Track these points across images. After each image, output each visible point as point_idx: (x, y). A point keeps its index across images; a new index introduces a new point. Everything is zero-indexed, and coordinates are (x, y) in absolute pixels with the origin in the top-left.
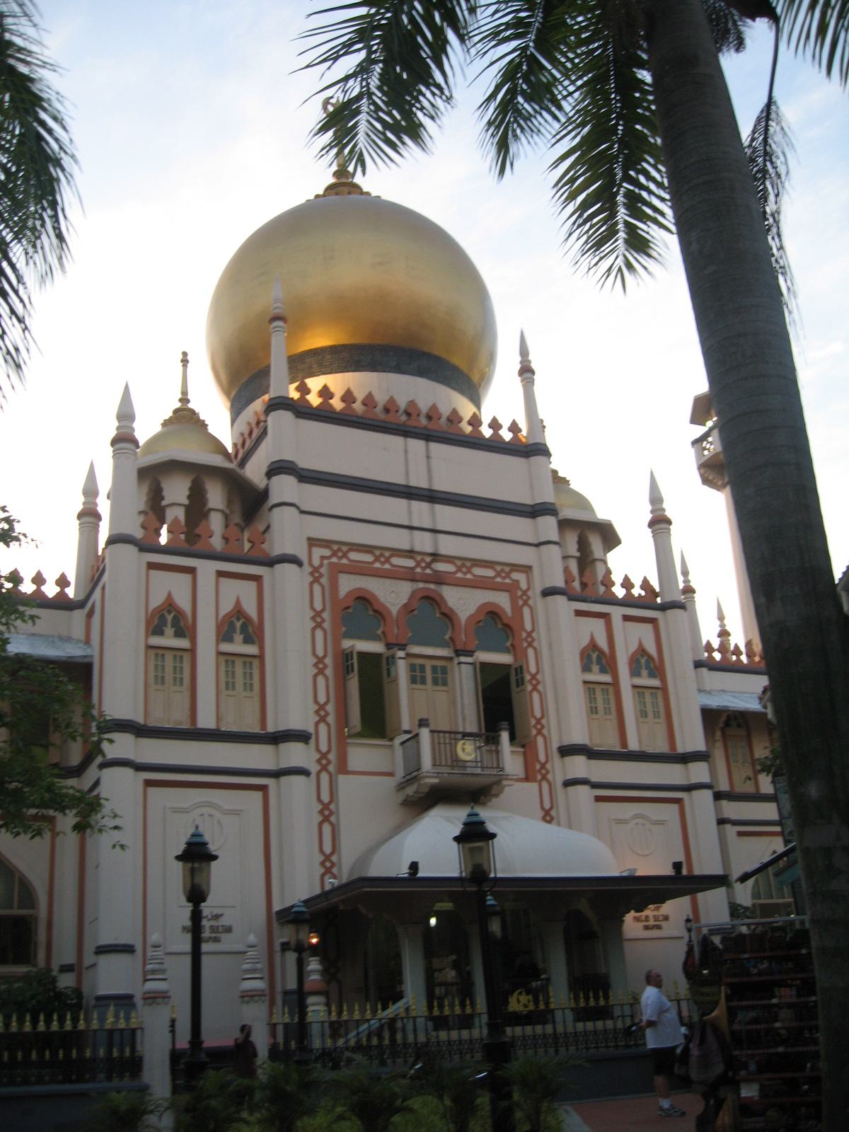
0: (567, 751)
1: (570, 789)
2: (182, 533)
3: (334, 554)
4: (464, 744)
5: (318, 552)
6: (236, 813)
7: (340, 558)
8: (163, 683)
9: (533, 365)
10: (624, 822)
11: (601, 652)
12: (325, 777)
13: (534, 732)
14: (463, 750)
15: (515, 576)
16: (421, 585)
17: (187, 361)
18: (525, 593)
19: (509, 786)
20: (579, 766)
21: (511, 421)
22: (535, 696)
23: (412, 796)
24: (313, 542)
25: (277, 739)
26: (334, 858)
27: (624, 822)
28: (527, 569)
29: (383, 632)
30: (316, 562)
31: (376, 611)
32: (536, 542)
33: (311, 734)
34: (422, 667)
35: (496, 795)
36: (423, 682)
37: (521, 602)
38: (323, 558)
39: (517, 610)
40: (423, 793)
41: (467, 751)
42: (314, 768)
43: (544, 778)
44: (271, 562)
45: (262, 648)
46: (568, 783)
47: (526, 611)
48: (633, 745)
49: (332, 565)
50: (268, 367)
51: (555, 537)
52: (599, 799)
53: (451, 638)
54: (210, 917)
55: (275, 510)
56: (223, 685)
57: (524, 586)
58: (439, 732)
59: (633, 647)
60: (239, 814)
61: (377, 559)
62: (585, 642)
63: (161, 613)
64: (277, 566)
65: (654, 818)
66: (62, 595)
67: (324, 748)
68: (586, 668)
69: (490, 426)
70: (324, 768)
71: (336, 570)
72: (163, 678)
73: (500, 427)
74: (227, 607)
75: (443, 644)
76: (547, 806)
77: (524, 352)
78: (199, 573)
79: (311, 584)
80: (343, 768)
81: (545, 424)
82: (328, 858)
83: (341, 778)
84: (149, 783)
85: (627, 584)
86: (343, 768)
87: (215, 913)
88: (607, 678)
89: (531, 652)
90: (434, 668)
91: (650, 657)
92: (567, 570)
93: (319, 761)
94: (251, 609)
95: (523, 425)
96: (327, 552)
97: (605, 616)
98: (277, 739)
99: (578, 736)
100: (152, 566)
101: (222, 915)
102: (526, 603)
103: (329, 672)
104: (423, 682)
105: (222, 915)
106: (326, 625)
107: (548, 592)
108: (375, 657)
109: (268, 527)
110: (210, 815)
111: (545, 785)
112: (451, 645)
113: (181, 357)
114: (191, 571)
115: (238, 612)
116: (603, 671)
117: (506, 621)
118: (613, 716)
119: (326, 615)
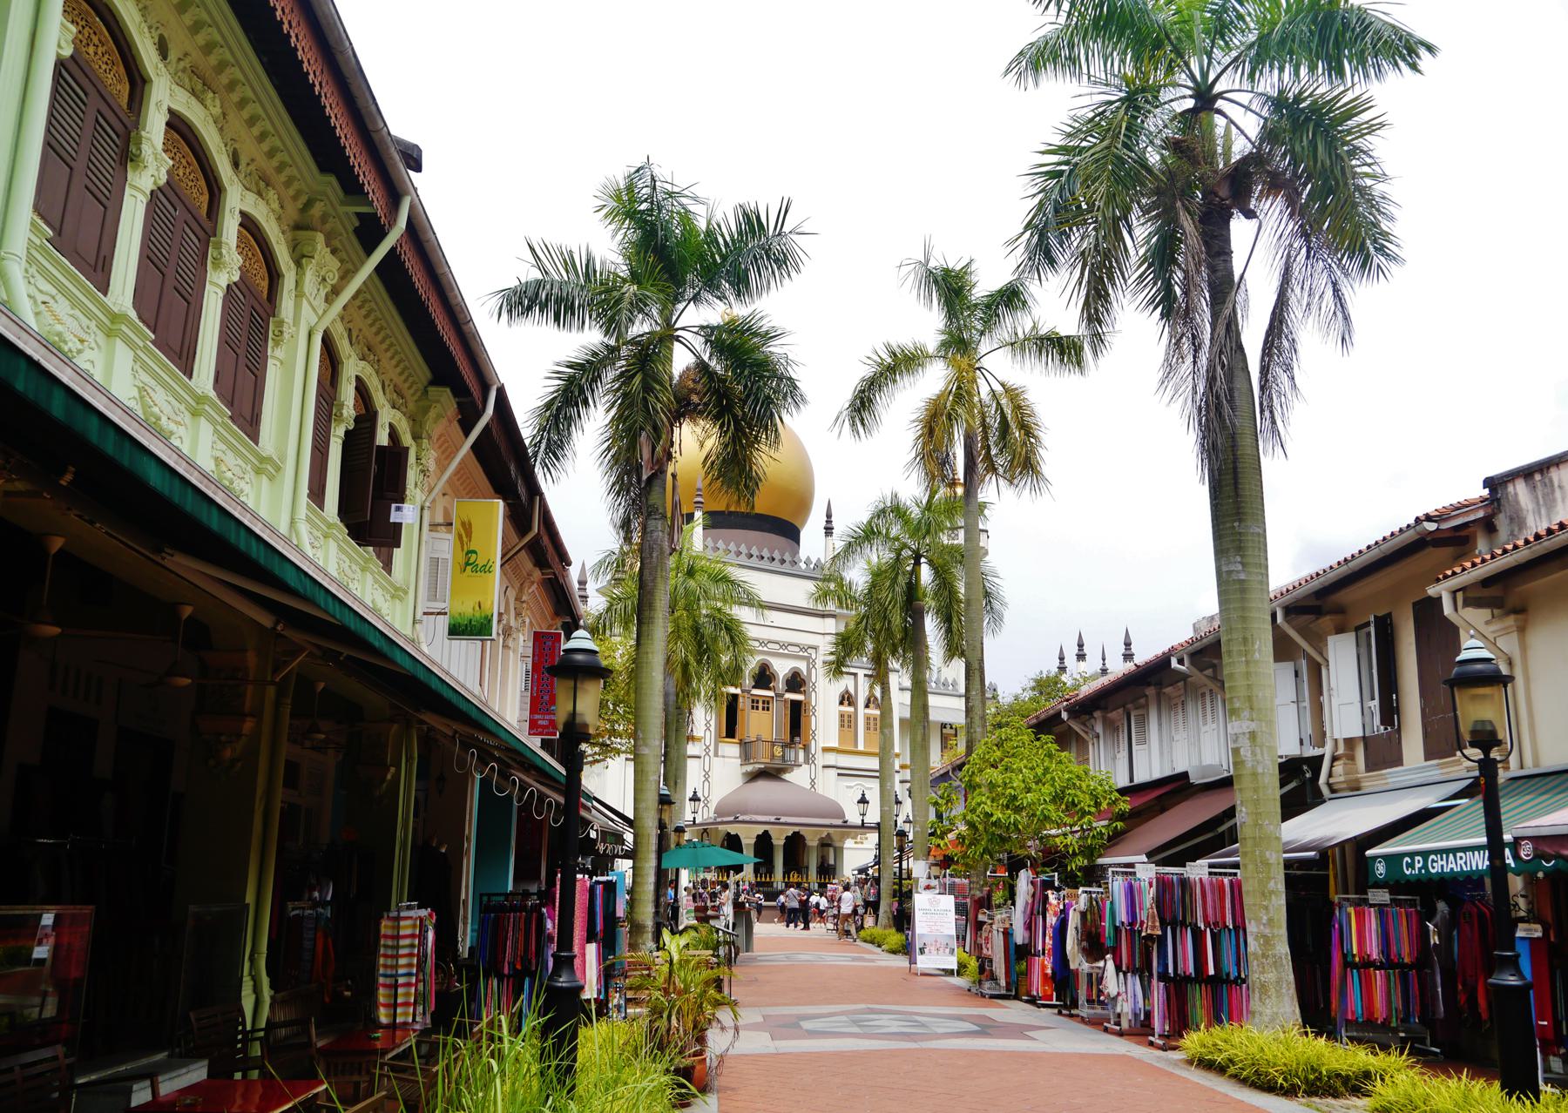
0: (826, 750)
1: (826, 770)
10: (851, 787)
11: (850, 697)
12: (707, 757)
20: (831, 759)
22: (813, 718)
27: (851, 787)
28: (815, 648)
34: (758, 702)
41: (778, 751)
46: (824, 767)
47: (813, 670)
48: (861, 747)
52: (839, 774)
57: (814, 657)
62: (842, 689)
68: (841, 703)
70: (707, 754)
75: (769, 689)
77: (829, 516)
80: (716, 755)
86: (716, 755)
88: (851, 709)
89: (813, 693)
97: (855, 675)
99: (835, 744)
108: (735, 697)
116: (849, 704)
118: (852, 729)
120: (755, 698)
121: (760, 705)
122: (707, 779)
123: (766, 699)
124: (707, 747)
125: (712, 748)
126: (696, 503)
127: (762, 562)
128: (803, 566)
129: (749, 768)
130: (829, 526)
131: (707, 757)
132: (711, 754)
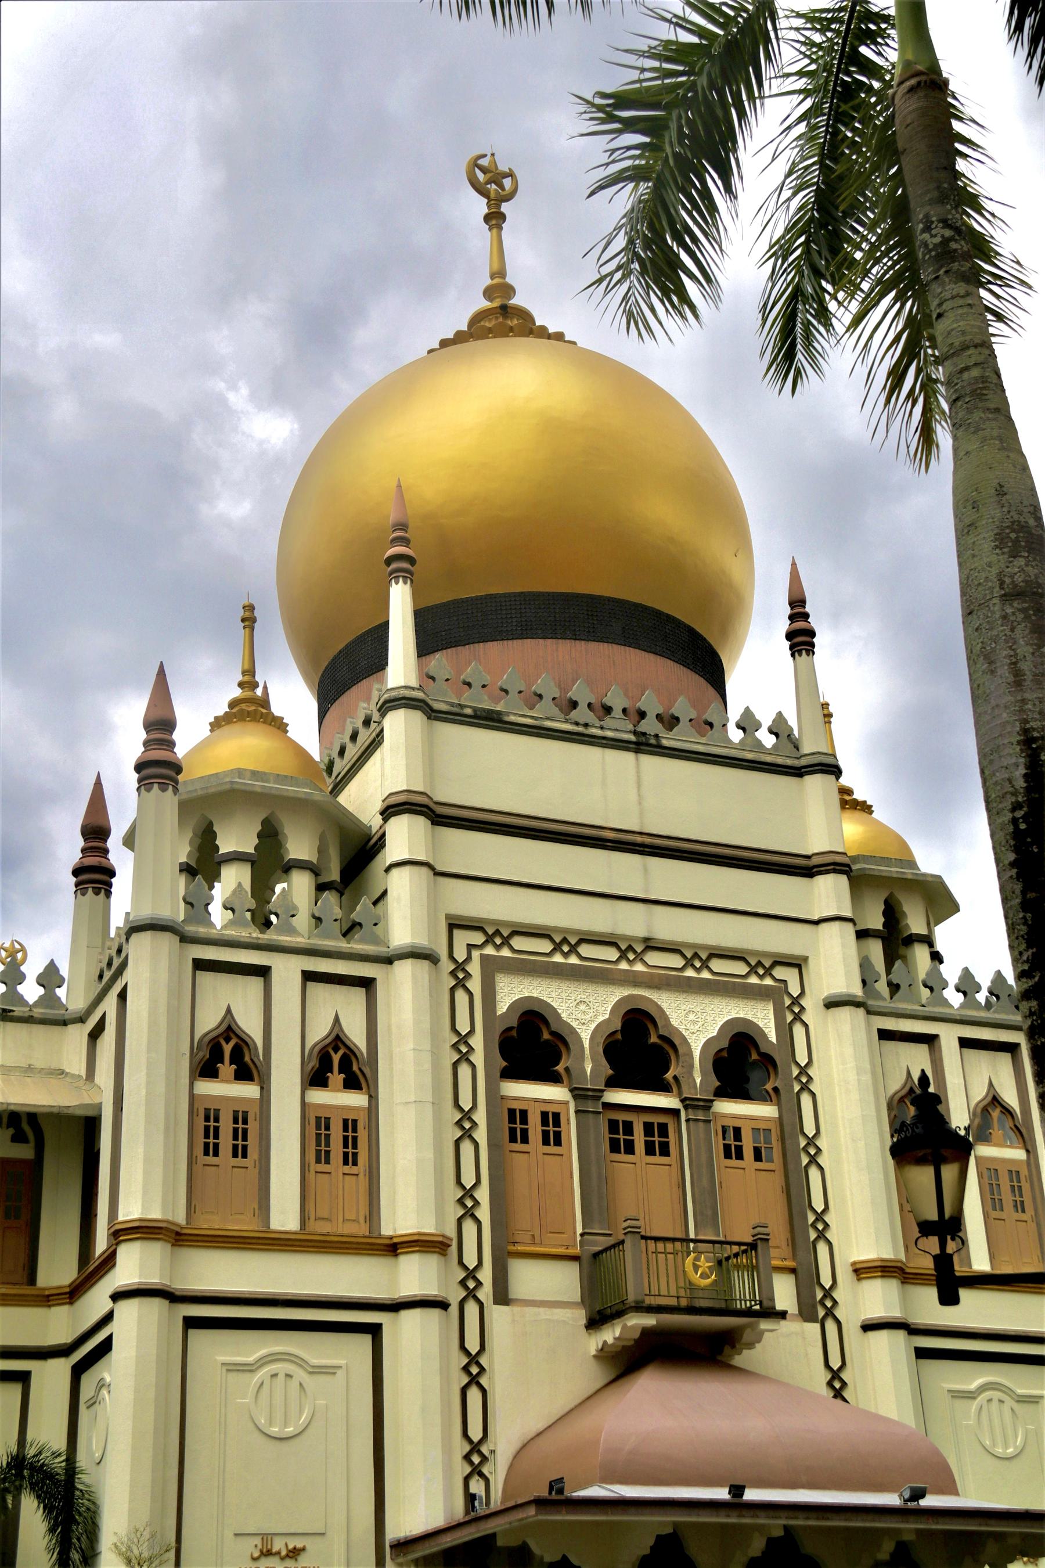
1: (872, 1335)
2: (248, 910)
3: (489, 940)
4: (697, 1259)
5: (463, 939)
6: (329, 1371)
7: (498, 947)
8: (216, 1154)
9: (814, 622)
13: (813, 1235)
14: (696, 1268)
15: (780, 972)
16: (626, 992)
17: (254, 620)
18: (796, 1001)
19: (772, 1331)
21: (774, 716)
22: (814, 1173)
23: (612, 1345)
24: (454, 925)
25: (393, 1248)
26: (484, 1449)
28: (798, 964)
29: (567, 1069)
30: (460, 955)
31: (554, 1034)
32: (816, 918)
33: (451, 1240)
34: (628, 1127)
35: (751, 1346)
36: (630, 1149)
37: (789, 1018)
38: (470, 947)
39: (785, 1032)
40: (629, 1340)
42: (454, 1295)
43: (830, 1313)
44: (388, 960)
45: (373, 1098)
46: (868, 1327)
47: (798, 1031)
49: (484, 958)
50: (385, 626)
51: (848, 913)
52: (922, 1353)
53: (675, 1078)
54: (284, 1553)
55: (395, 872)
56: (311, 1156)
57: (795, 991)
58: (656, 1239)
59: (979, 1093)
60: (334, 1373)
61: (557, 948)
63: (216, 1041)
64: (396, 963)
65: (1020, 1391)
66: (49, 999)
67: (471, 1262)
69: (739, 726)
70: (471, 1294)
71: (491, 968)
72: (216, 1146)
73: (758, 726)
74: (319, 1031)
75: (663, 1088)
76: (836, 1364)
78: (275, 976)
79: (452, 990)
80: (502, 1297)
81: (831, 709)
82: (475, 1448)
83: (497, 1314)
84: (191, 1323)
85: (967, 985)
86: (502, 1297)
87: (291, 1547)
90: (648, 1128)
91: (1007, 1111)
92: (865, 965)
93: (463, 1283)
94: (356, 1034)
95: (793, 721)
96: (478, 938)
97: (929, 1040)
98: (393, 1248)
100: (200, 965)
101: (304, 1549)
102: (797, 1018)
103: (481, 1135)
104: (630, 1149)
105: (304, 1549)
106: (478, 1058)
107: (832, 1004)
109: (385, 893)
110: (288, 1376)
111: (831, 1326)
112: (675, 1089)
113: (241, 613)
114: (263, 972)
115: (337, 1040)
117: (764, 1049)
119: (477, 1041)
120: (621, 1117)
121: (639, 1138)
122: (474, 1380)
123: (656, 1119)
124: (471, 1274)
125: (486, 1275)
126: (389, 561)
127: (608, 722)
128: (735, 735)
129: (610, 1334)
130: (800, 625)
131: (471, 1309)
132: (486, 1293)
